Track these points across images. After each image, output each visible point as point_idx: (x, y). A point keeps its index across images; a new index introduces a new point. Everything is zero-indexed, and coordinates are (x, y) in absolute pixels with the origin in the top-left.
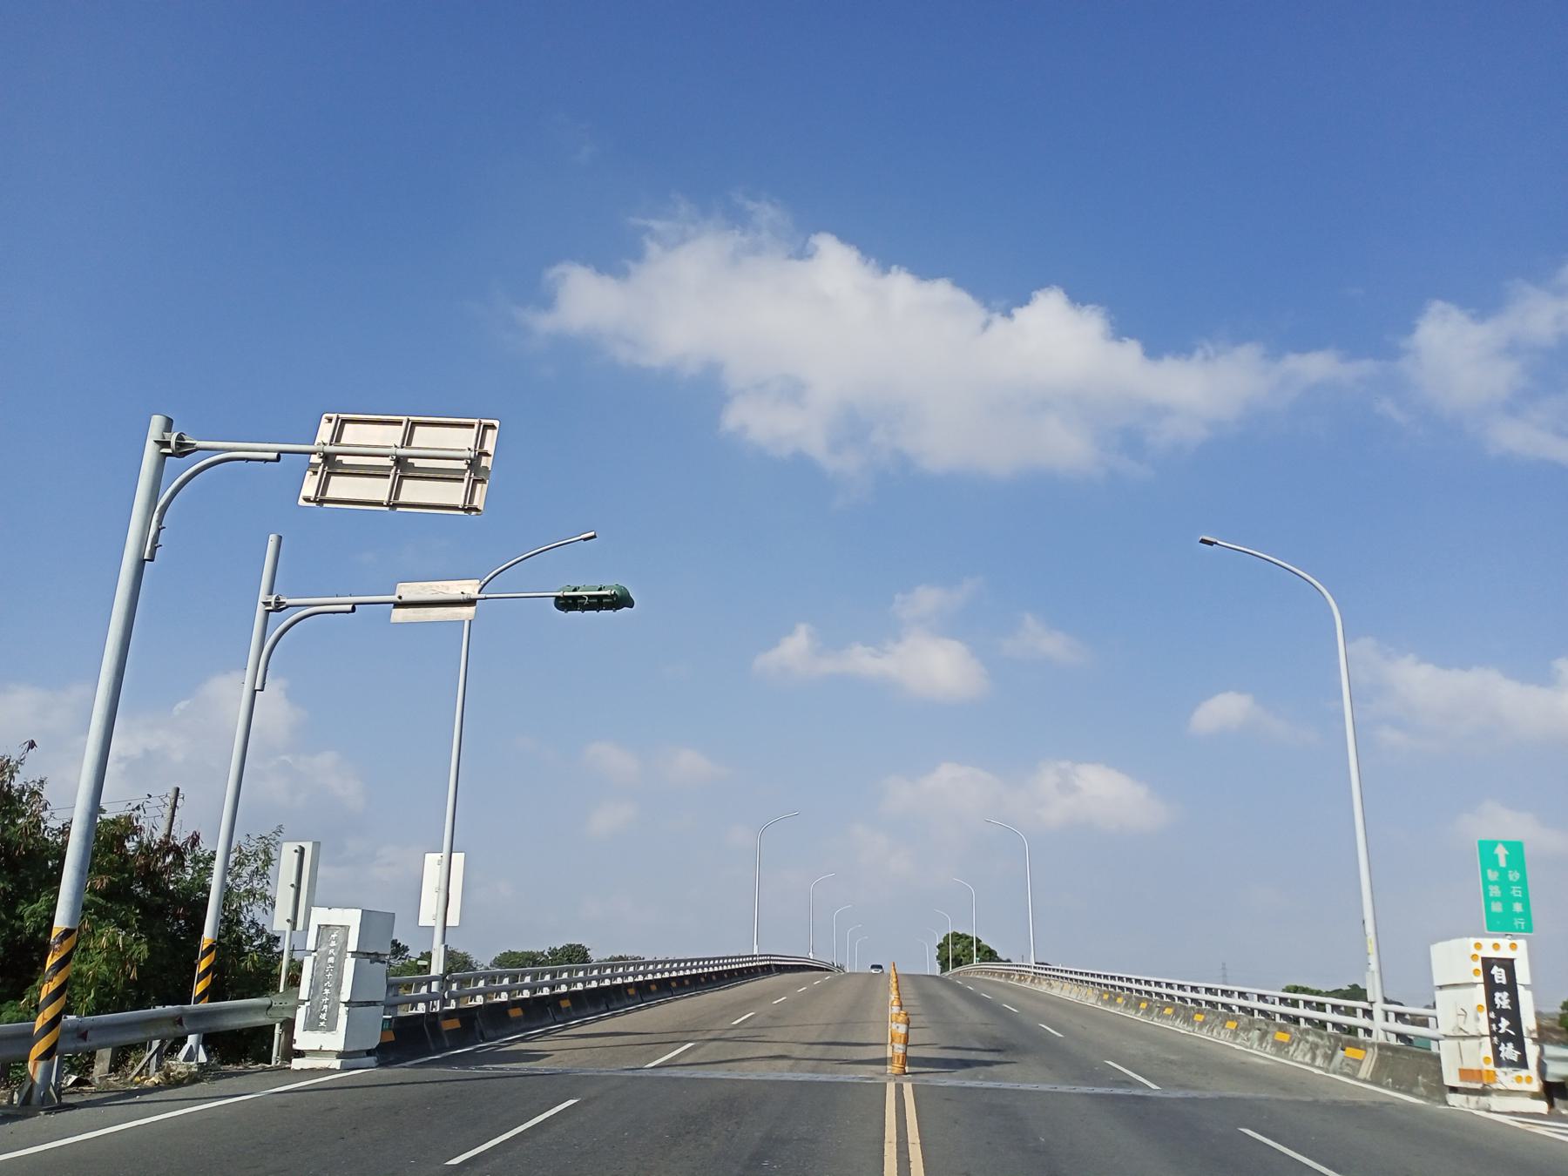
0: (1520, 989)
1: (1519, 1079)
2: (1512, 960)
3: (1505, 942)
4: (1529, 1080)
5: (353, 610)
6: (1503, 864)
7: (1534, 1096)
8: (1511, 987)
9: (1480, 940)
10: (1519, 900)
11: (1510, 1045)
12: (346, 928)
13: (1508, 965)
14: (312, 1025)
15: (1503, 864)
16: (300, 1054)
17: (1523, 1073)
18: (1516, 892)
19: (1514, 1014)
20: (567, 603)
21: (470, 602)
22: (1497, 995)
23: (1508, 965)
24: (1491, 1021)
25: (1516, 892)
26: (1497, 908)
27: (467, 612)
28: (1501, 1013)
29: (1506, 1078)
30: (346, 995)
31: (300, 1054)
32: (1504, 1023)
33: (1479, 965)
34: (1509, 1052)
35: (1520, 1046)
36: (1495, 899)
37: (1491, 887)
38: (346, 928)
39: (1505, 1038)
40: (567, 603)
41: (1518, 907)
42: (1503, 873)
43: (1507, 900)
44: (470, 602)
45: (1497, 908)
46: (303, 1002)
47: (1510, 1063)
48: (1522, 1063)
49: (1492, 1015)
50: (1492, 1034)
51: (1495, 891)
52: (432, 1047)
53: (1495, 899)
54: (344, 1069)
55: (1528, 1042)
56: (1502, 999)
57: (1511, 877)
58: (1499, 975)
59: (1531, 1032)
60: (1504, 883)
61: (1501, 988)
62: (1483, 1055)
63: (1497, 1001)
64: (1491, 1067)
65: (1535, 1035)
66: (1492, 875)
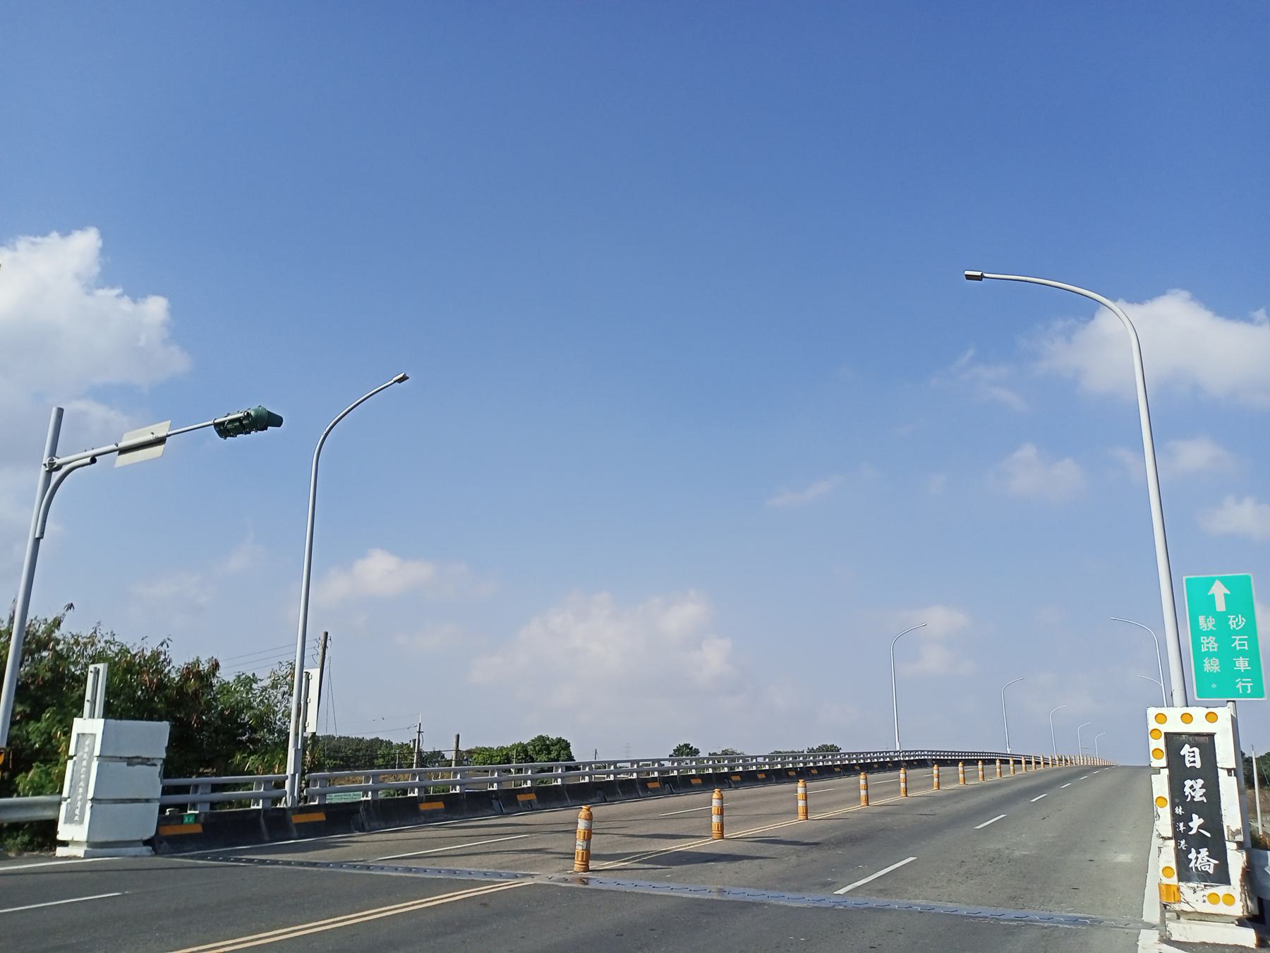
0: (1222, 774)
1: (1214, 899)
2: (1211, 736)
3: (1198, 713)
4: (1229, 900)
5: (93, 460)
6: (1221, 606)
7: (1242, 922)
8: (1209, 772)
9: (1163, 710)
10: (1242, 654)
11: (1204, 852)
12: (94, 735)
13: (1206, 743)
14: (70, 819)
15: (1221, 606)
16: (65, 844)
17: (1221, 890)
18: (1238, 643)
19: (1211, 809)
20: (224, 430)
21: (161, 441)
22: (1188, 783)
23: (1206, 743)
24: (1176, 819)
25: (1238, 643)
26: (1212, 666)
27: (158, 450)
28: (1192, 807)
29: (1194, 897)
30: (90, 795)
31: (65, 844)
32: (1196, 821)
33: (1160, 744)
34: (1202, 860)
35: (1219, 853)
36: (1210, 655)
37: (1203, 639)
38: (94, 735)
39: (1198, 842)
40: (224, 430)
41: (1242, 664)
42: (1221, 619)
43: (1226, 654)
44: (161, 441)
45: (1212, 666)
46: (65, 800)
47: (1204, 877)
48: (1222, 876)
49: (1179, 811)
50: (1177, 836)
51: (1209, 644)
52: (266, 838)
53: (1210, 655)
54: (87, 855)
55: (1231, 846)
56: (1195, 789)
57: (1232, 624)
58: (1192, 756)
59: (1234, 834)
60: (1222, 632)
61: (1193, 774)
62: (1162, 865)
63: (1187, 790)
64: (1174, 880)
65: (1240, 838)
66: (1205, 623)
